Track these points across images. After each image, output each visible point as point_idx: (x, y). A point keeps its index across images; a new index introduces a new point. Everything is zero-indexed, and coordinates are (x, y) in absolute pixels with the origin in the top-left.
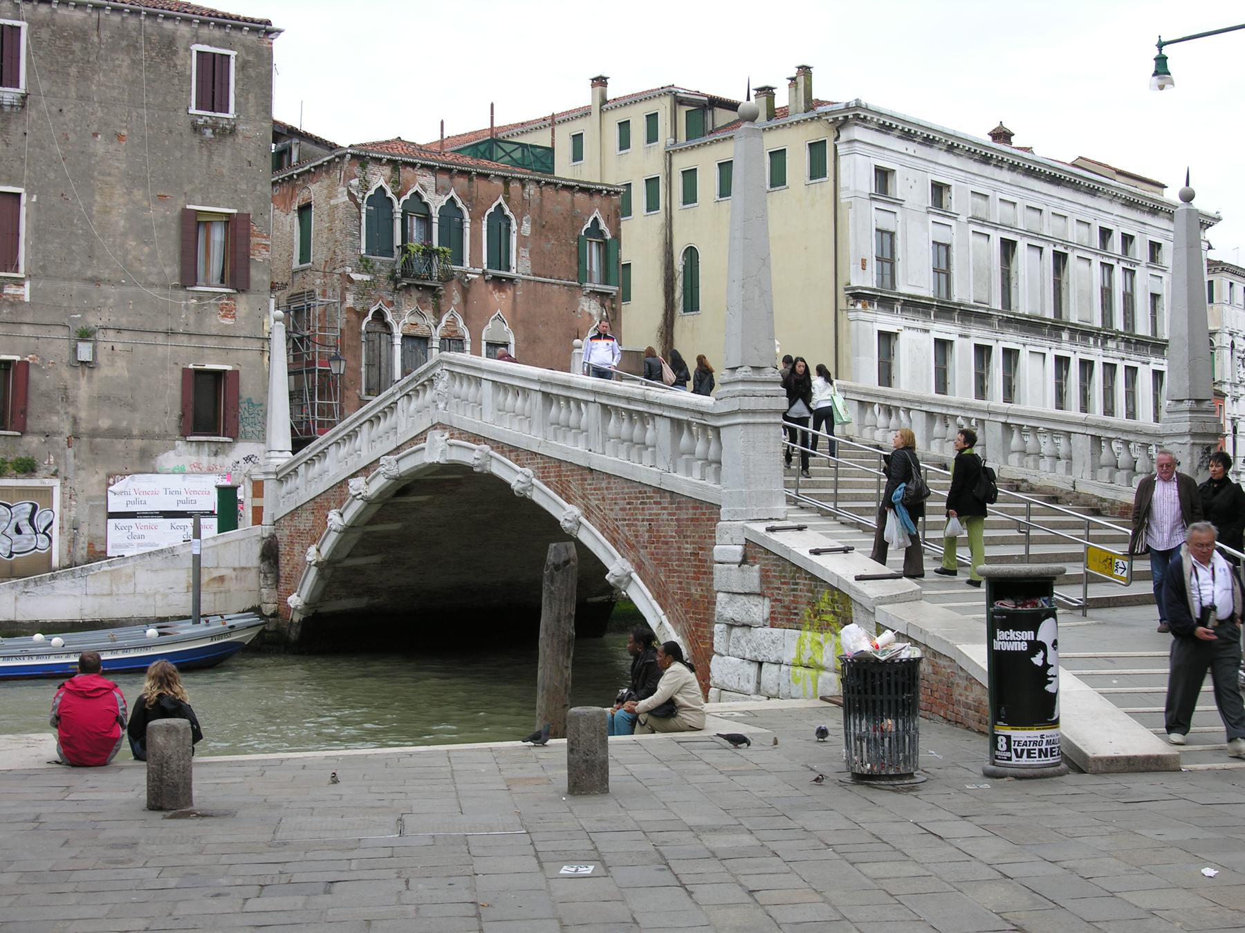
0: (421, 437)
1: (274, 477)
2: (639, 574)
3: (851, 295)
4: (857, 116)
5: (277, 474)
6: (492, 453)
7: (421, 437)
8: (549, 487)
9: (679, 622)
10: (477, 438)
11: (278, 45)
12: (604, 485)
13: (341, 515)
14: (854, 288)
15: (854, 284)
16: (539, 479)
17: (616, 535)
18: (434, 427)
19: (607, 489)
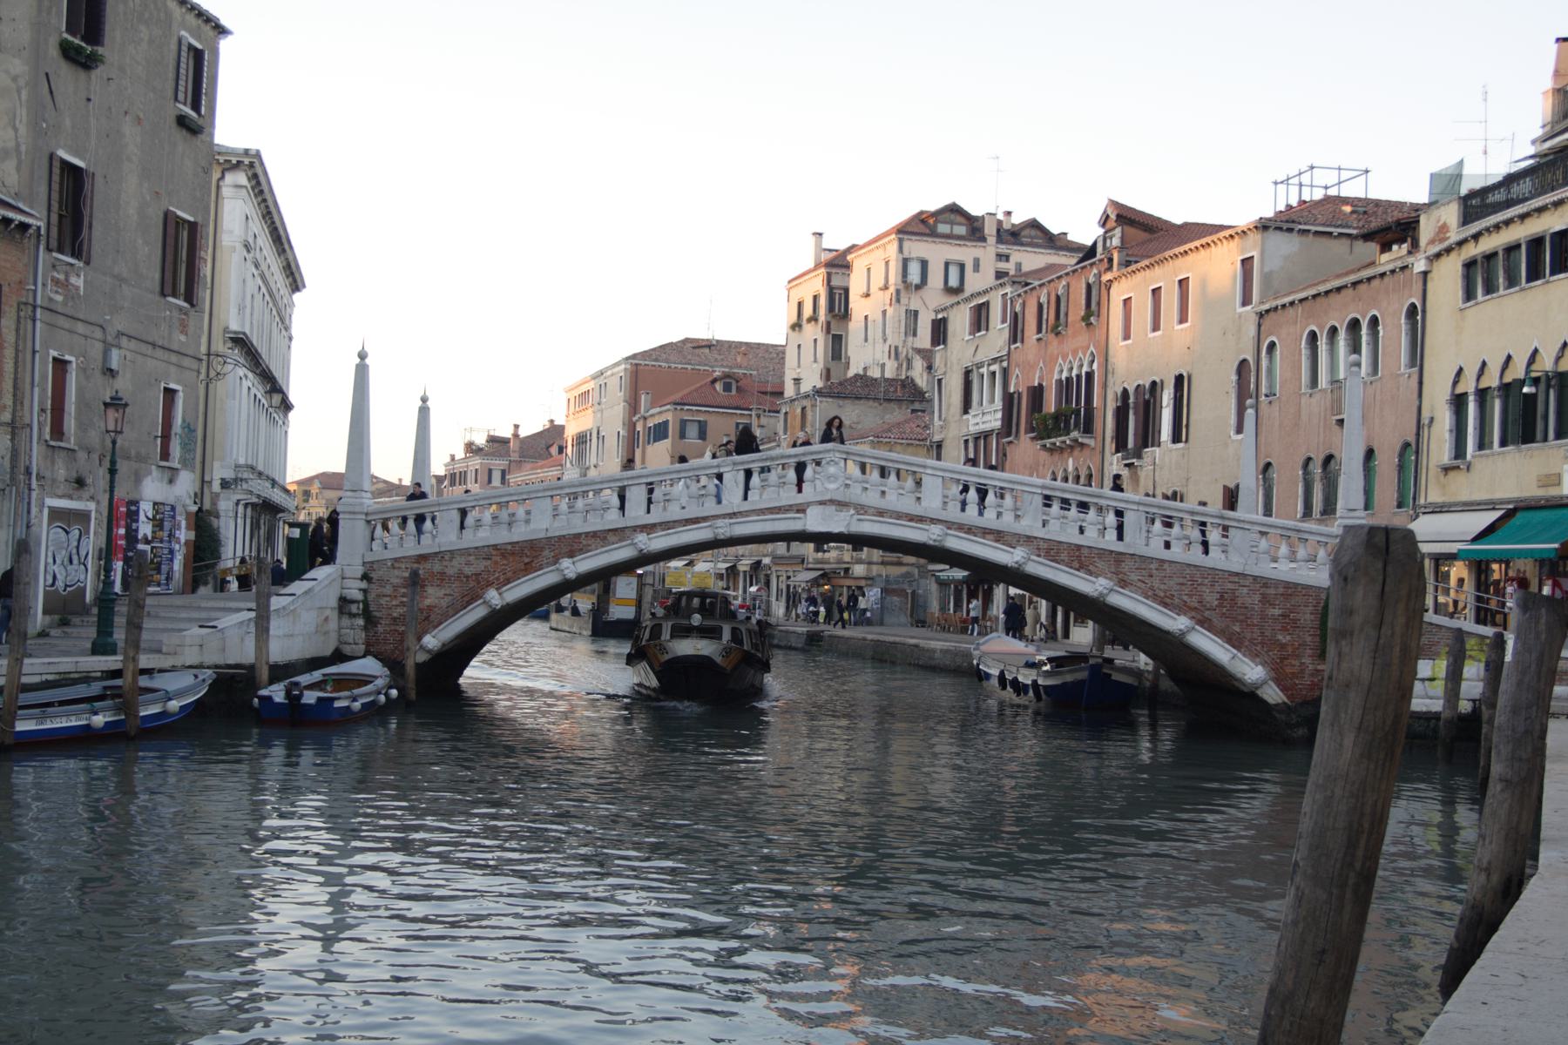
0: (801, 509)
1: (364, 517)
2: (1202, 626)
3: (231, 338)
4: (251, 165)
5: (367, 514)
6: (950, 532)
7: (801, 509)
8: (1059, 563)
9: (1257, 656)
10: (920, 519)
11: (225, 45)
12: (1152, 566)
13: (574, 563)
14: (235, 333)
15: (234, 326)
16: (1039, 556)
17: (1168, 601)
18: (822, 503)
19: (1157, 569)
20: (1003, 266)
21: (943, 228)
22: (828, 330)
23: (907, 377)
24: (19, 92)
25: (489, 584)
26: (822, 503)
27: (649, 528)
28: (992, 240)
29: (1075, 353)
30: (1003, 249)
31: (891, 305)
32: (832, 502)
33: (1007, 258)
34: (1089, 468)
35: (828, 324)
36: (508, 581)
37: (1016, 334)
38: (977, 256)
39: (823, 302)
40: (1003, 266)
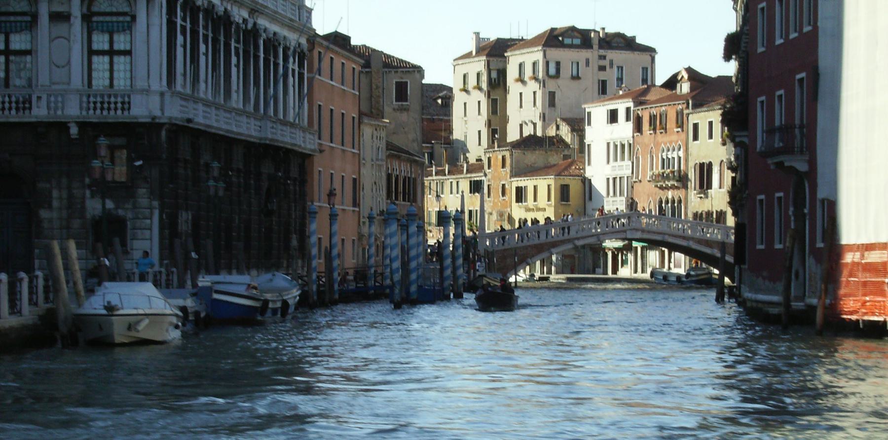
18: (631, 230)
20: (602, 63)
21: (568, 41)
22: (489, 97)
23: (557, 135)
24: (417, 123)
25: (528, 257)
26: (631, 230)
27: (578, 239)
28: (596, 47)
29: (671, 143)
30: (602, 52)
31: (540, 88)
32: (634, 229)
33: (604, 57)
34: (680, 197)
35: (489, 92)
36: (533, 256)
37: (638, 128)
38: (588, 57)
39: (484, 78)
40: (602, 63)
